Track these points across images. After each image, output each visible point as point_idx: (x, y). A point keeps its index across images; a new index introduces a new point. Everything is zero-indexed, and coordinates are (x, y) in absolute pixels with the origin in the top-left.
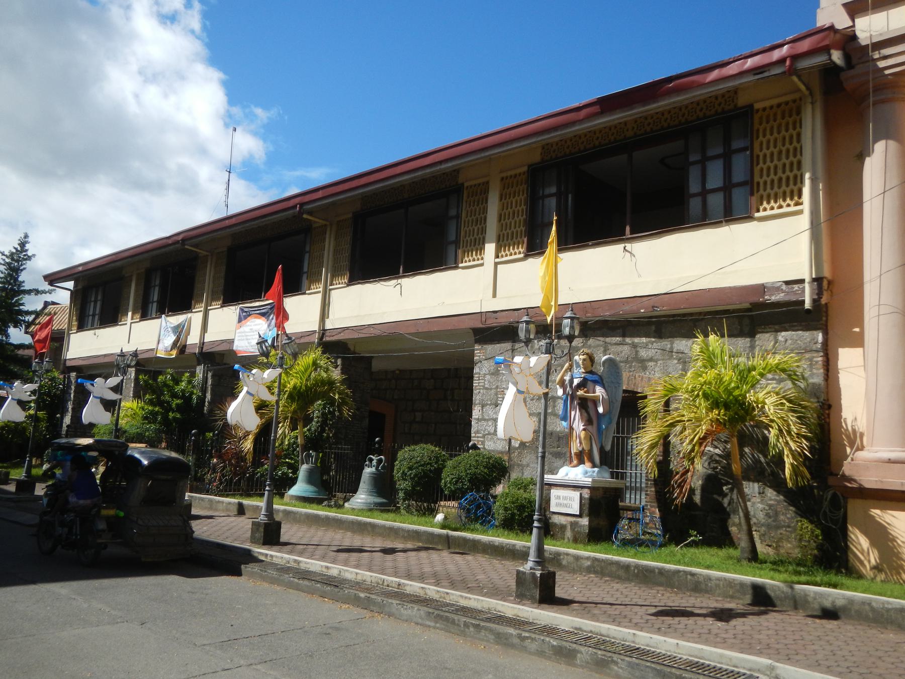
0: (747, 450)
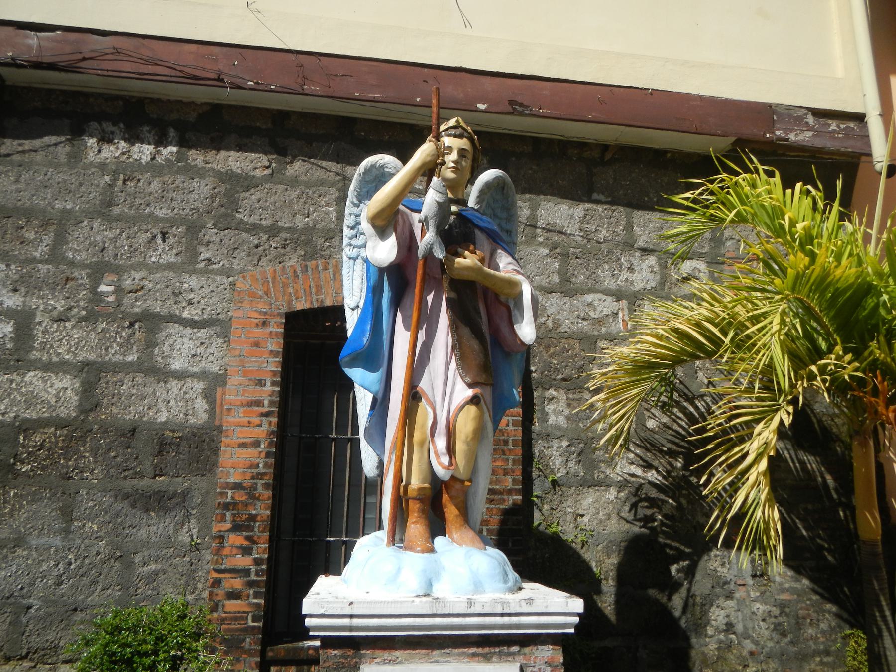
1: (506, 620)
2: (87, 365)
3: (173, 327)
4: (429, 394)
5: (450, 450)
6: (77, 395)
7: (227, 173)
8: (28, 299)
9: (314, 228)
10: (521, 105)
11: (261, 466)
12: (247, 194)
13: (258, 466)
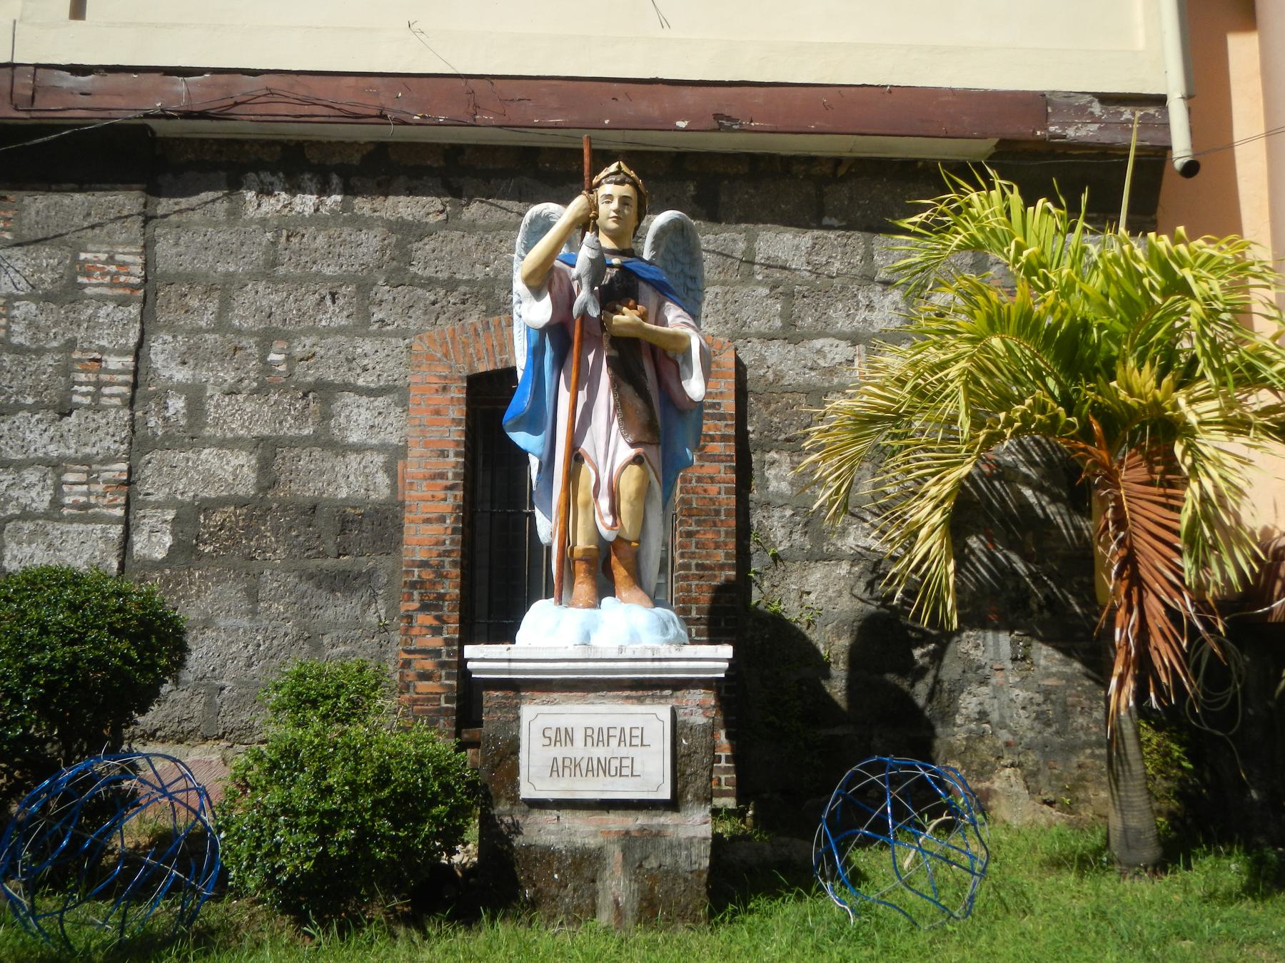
0: (974, 542)
1: (657, 665)
2: (262, 440)
3: (348, 395)
4: (592, 455)
5: (615, 510)
6: (254, 472)
7: (397, 221)
8: (197, 372)
9: (495, 279)
10: (729, 118)
11: (447, 542)
12: (420, 244)
13: (444, 543)
